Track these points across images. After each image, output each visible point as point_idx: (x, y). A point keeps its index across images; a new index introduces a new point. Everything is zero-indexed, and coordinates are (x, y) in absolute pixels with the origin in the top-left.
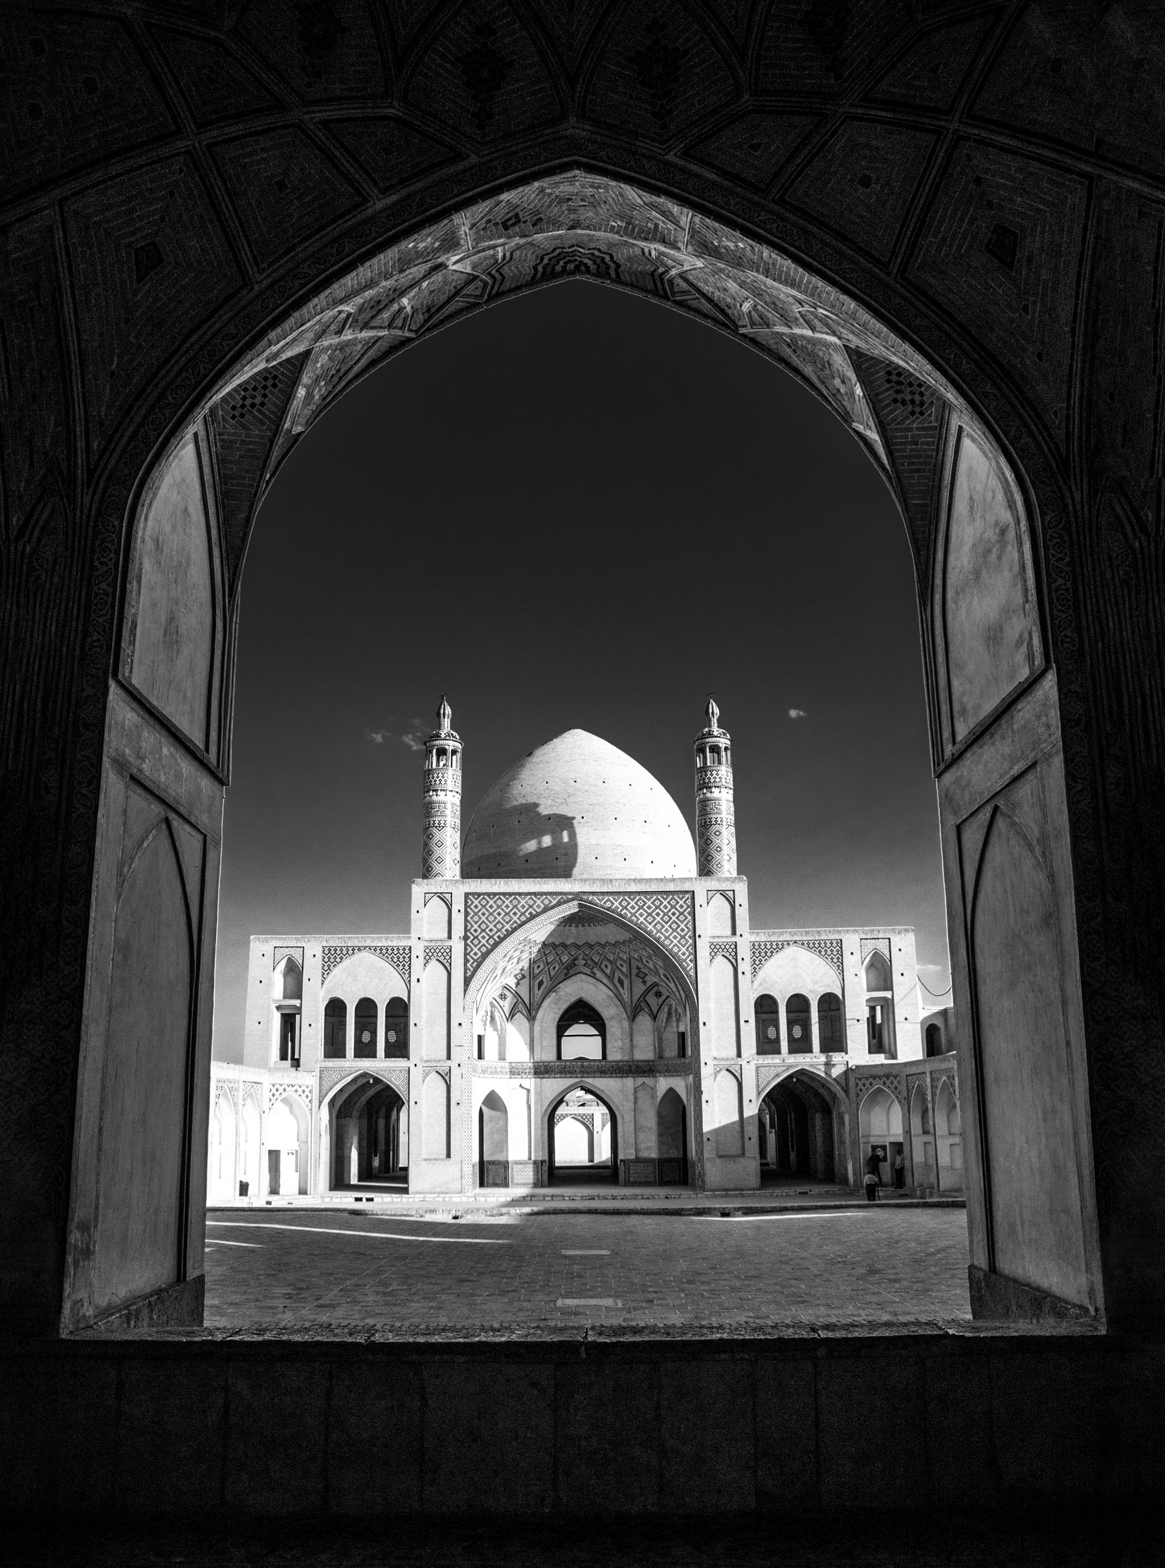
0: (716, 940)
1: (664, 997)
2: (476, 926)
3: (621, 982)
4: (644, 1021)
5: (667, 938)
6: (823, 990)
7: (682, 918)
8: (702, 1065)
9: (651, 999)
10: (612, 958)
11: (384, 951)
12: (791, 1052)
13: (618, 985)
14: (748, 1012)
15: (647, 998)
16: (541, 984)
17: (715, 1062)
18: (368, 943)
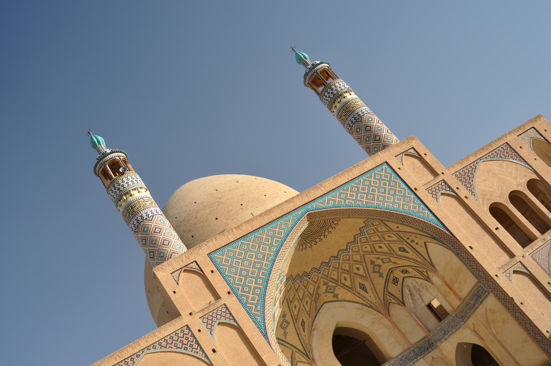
0: (429, 186)
1: (400, 281)
2: (237, 277)
3: (363, 287)
4: (396, 310)
5: (393, 203)
6: (524, 181)
7: (392, 184)
8: (495, 278)
9: (393, 289)
10: (347, 268)
11: (164, 344)
12: (542, 233)
13: (361, 291)
14: (492, 222)
15: (389, 290)
17: (502, 270)
18: (143, 344)
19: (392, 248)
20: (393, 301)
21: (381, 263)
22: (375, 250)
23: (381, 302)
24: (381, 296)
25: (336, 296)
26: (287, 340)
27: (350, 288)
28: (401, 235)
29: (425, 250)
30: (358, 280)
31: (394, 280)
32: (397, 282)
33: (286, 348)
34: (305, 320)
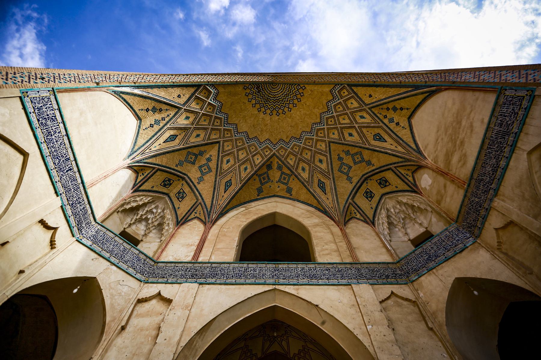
13: (318, 190)
16: (228, 184)
19: (364, 135)
20: (358, 216)
21: (352, 164)
22: (344, 138)
23: (339, 208)
24: (342, 202)
25: (289, 191)
26: (199, 187)
27: (305, 181)
28: (376, 112)
29: (409, 132)
30: (318, 176)
31: (366, 192)
32: (372, 197)
33: (192, 193)
34: (233, 182)
